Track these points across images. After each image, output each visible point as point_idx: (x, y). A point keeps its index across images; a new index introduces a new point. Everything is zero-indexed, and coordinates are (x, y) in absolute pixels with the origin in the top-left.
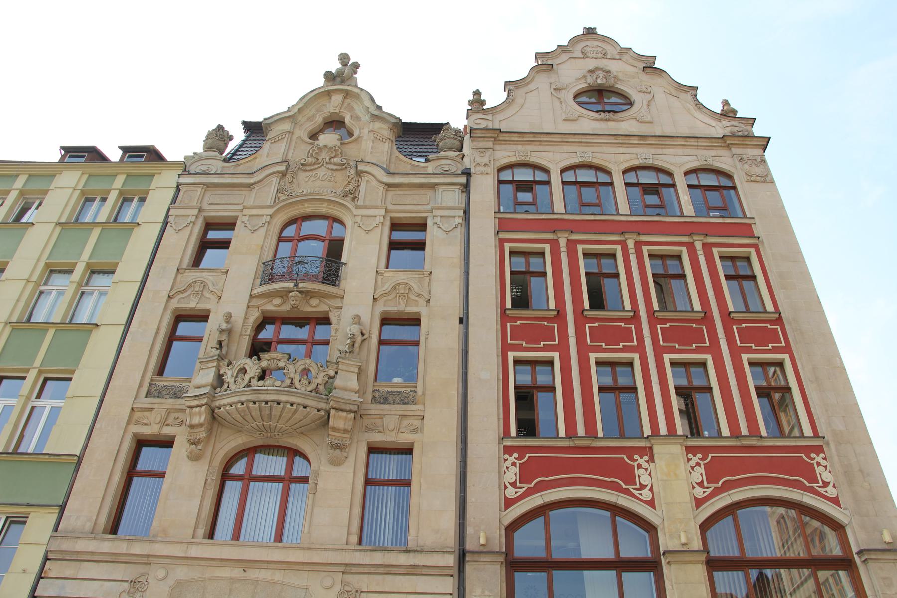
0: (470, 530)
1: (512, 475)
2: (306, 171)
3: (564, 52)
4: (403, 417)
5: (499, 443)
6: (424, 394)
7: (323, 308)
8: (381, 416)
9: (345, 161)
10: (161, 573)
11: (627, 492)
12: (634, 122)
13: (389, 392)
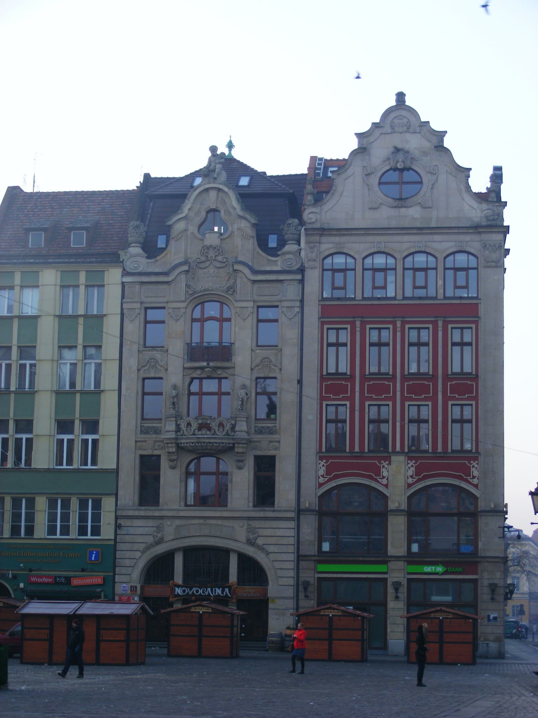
0: (302, 500)
1: (322, 472)
2: (201, 268)
3: (377, 127)
4: (271, 442)
5: (316, 455)
6: (280, 428)
8: (259, 442)
9: (225, 260)
10: (169, 523)
11: (376, 480)
12: (418, 208)
13: (262, 427)
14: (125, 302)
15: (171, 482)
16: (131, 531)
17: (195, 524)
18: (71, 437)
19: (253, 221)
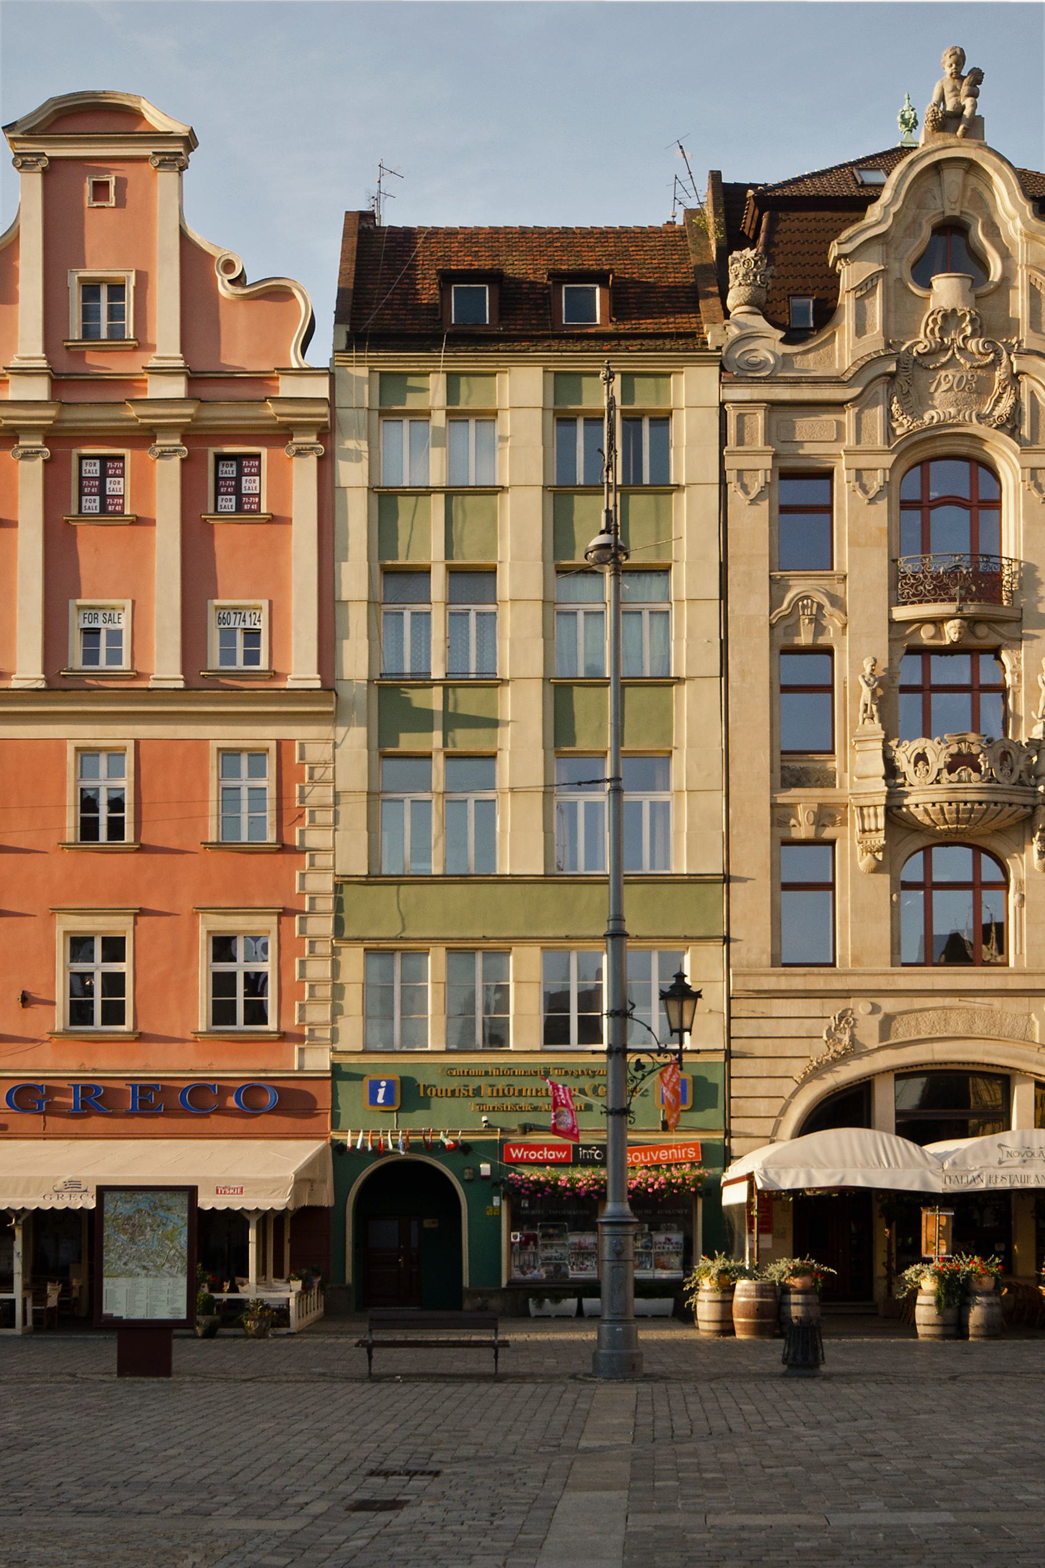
7: (993, 640)
14: (732, 453)
16: (767, 1027)
17: (934, 1009)
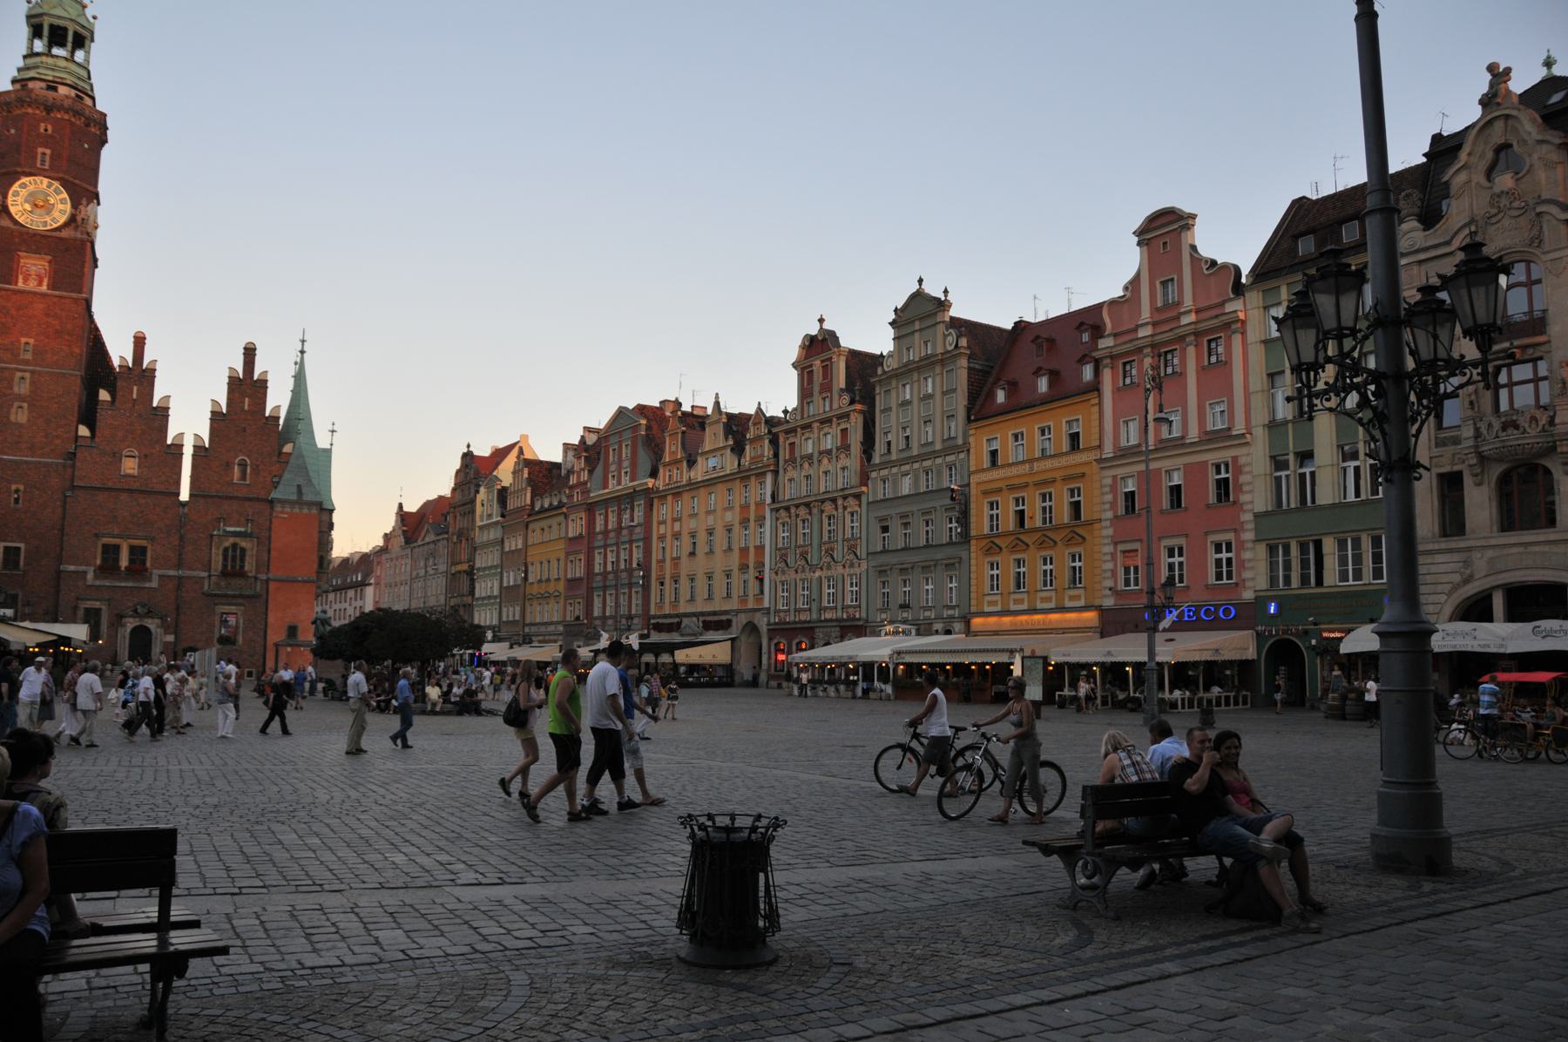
7: (1538, 354)
15: (1480, 503)
16: (1433, 569)
18: (1357, 463)
19: (1558, 141)
